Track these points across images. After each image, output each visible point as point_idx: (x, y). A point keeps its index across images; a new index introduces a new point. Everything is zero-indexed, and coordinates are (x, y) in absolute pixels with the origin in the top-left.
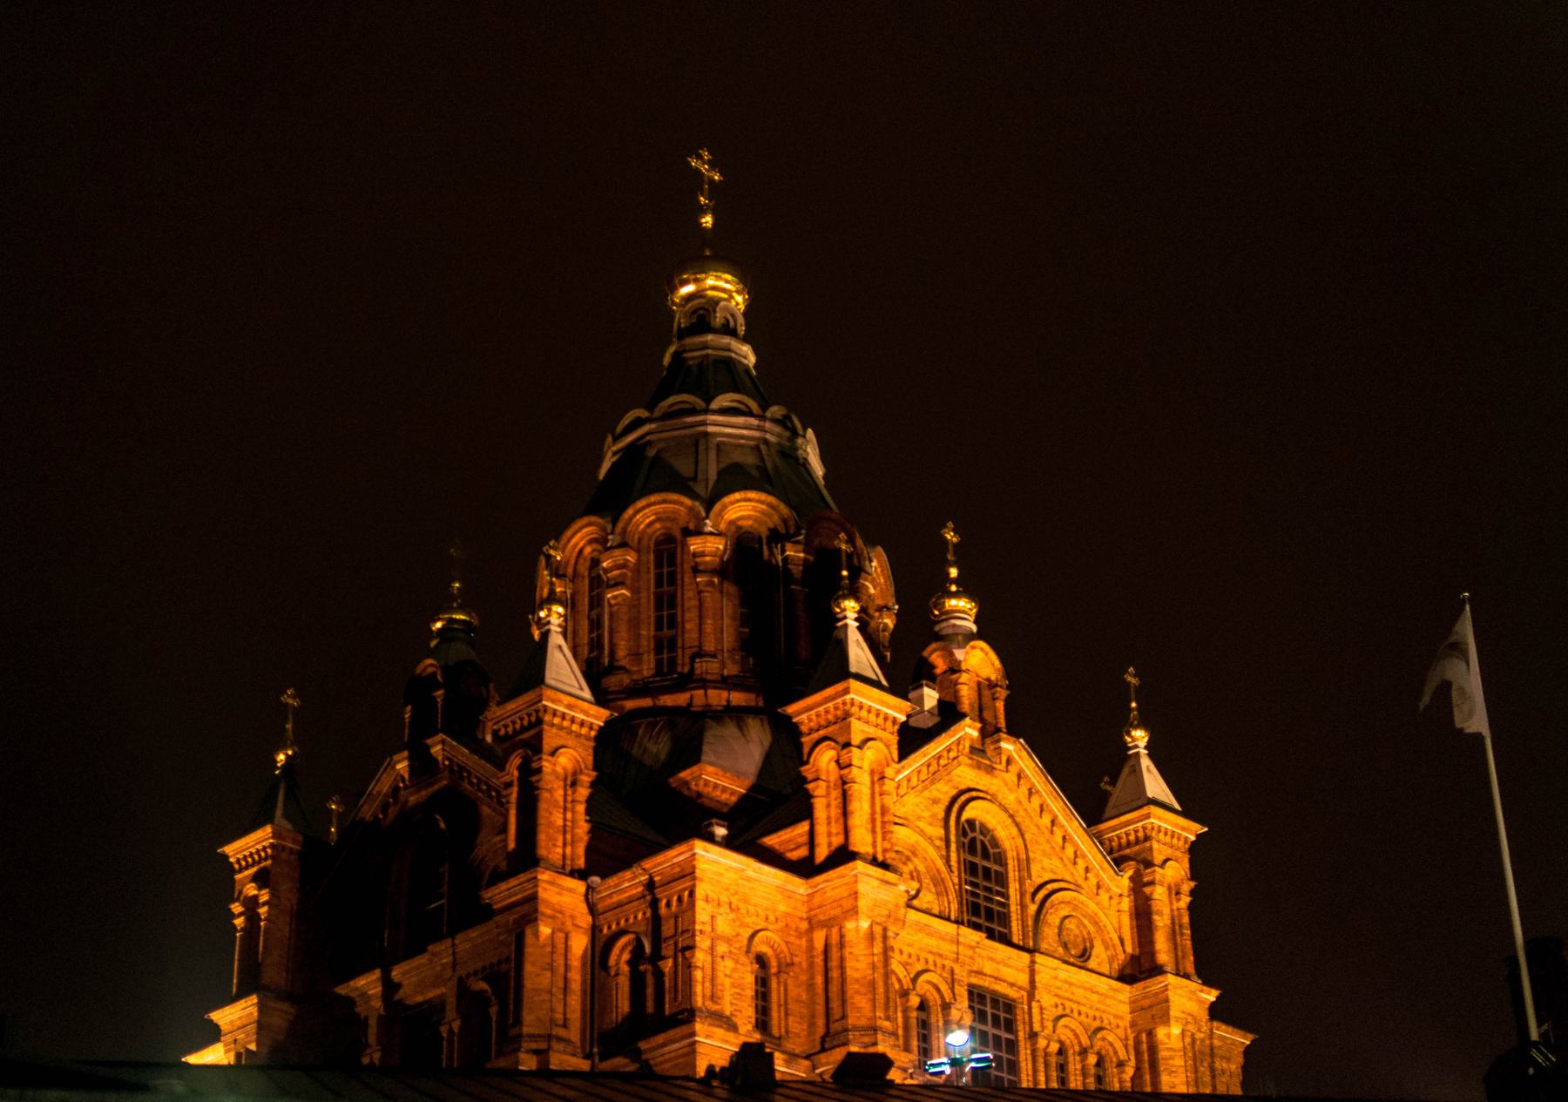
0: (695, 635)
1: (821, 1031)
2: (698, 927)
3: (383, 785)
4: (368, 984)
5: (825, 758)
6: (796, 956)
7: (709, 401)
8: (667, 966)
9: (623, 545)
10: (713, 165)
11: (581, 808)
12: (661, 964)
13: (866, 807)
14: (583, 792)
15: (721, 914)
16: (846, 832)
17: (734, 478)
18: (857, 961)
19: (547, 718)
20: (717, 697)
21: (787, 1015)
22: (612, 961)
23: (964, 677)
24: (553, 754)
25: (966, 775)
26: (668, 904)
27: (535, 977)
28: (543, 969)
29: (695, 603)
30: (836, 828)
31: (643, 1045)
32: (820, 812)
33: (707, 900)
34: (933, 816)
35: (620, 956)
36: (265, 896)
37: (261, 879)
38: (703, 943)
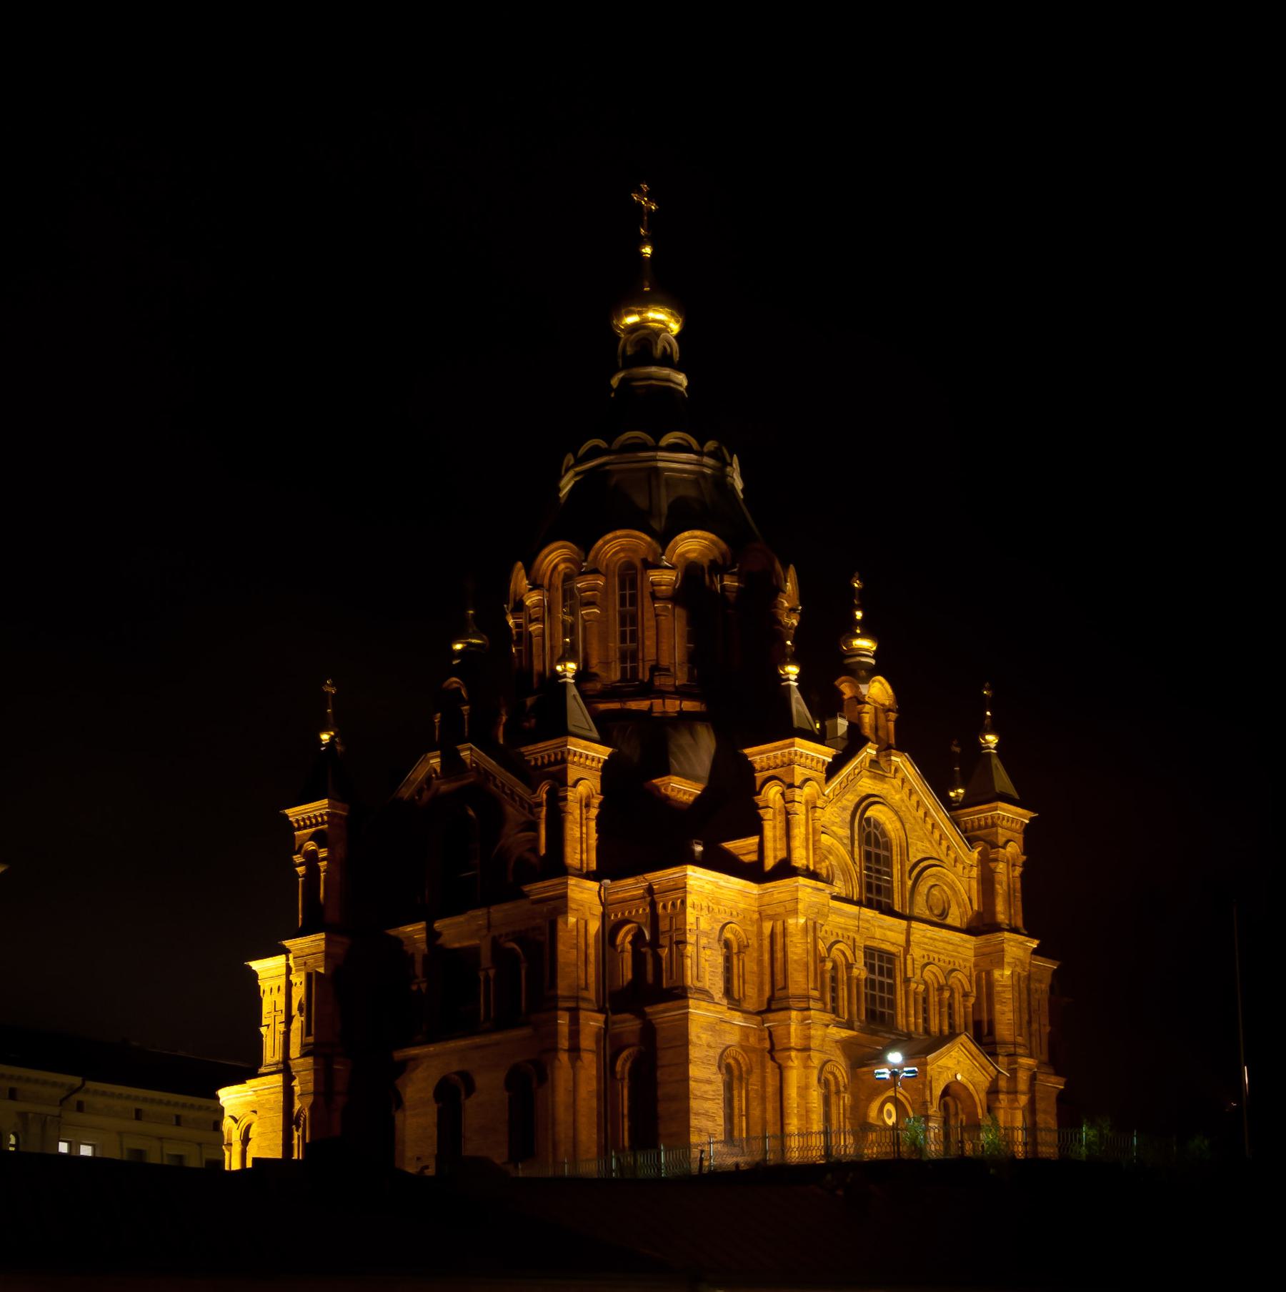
0: (654, 651)
1: (767, 993)
2: (688, 927)
3: (418, 774)
4: (414, 931)
5: (772, 793)
6: (750, 939)
7: (658, 438)
8: (664, 952)
9: (595, 571)
10: (652, 196)
11: (593, 824)
12: (659, 950)
13: (803, 830)
14: (594, 812)
15: (702, 916)
16: (789, 850)
17: (683, 518)
18: (796, 947)
19: (570, 758)
20: (673, 706)
21: (744, 983)
22: (619, 940)
23: (867, 708)
24: (575, 785)
25: (867, 785)
26: (665, 907)
27: (565, 953)
28: (572, 949)
29: (653, 623)
30: (781, 845)
31: (648, 1010)
32: (768, 832)
33: (693, 906)
34: (843, 820)
35: (625, 937)
36: (323, 853)
37: (319, 838)
38: (691, 938)
